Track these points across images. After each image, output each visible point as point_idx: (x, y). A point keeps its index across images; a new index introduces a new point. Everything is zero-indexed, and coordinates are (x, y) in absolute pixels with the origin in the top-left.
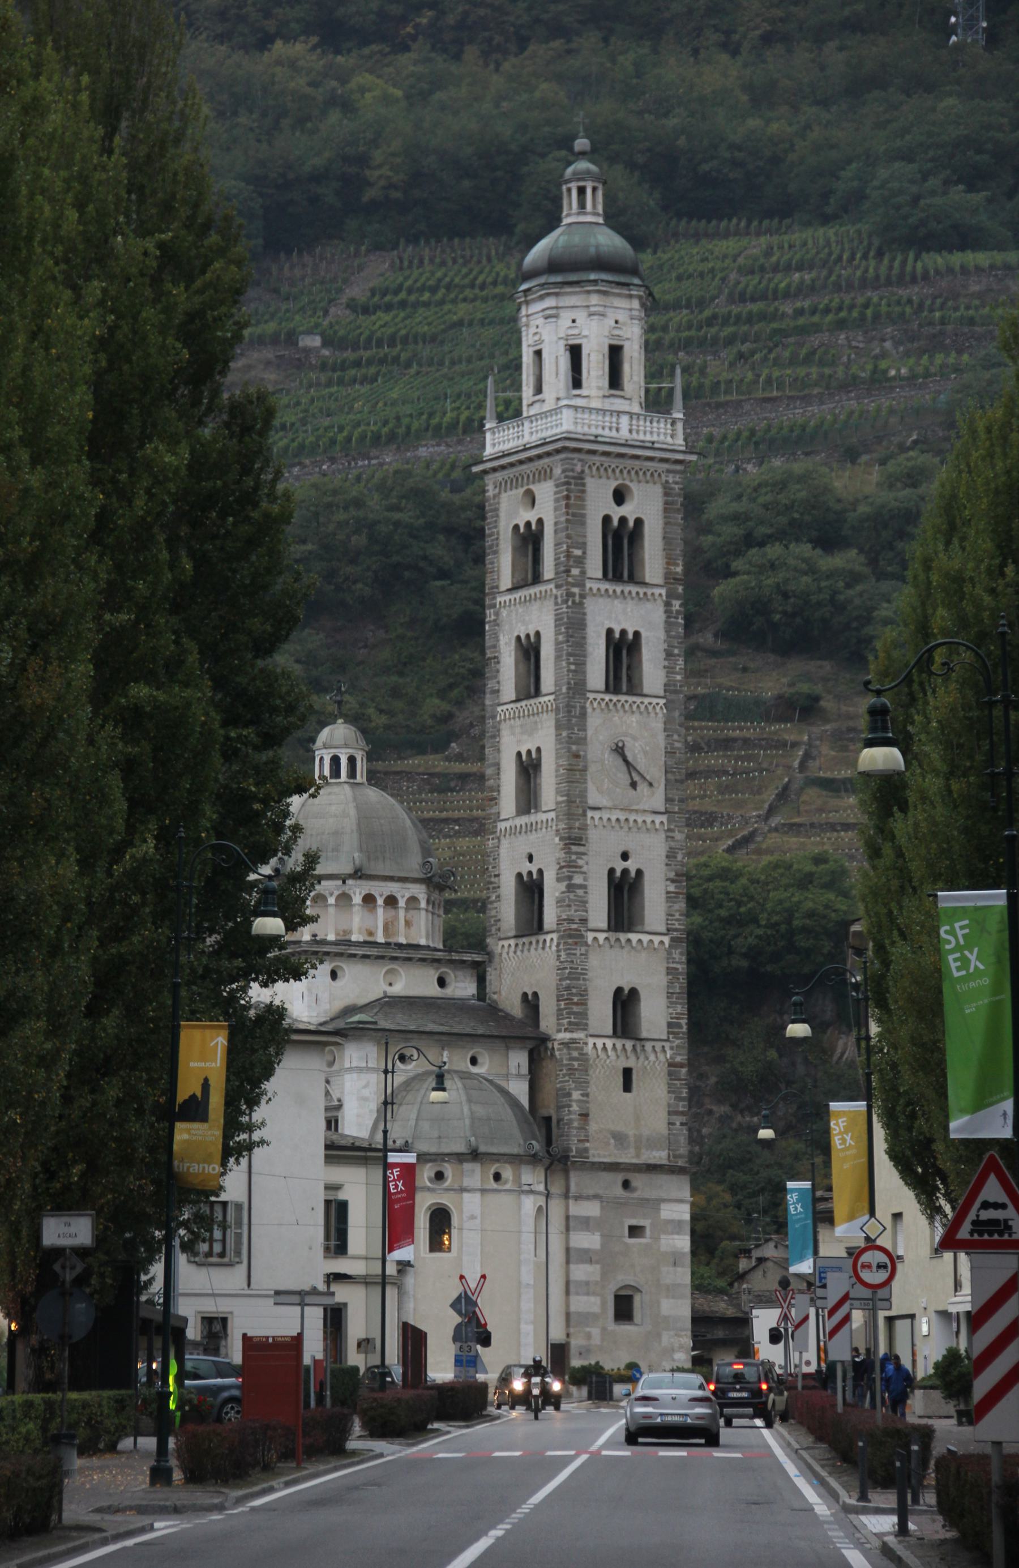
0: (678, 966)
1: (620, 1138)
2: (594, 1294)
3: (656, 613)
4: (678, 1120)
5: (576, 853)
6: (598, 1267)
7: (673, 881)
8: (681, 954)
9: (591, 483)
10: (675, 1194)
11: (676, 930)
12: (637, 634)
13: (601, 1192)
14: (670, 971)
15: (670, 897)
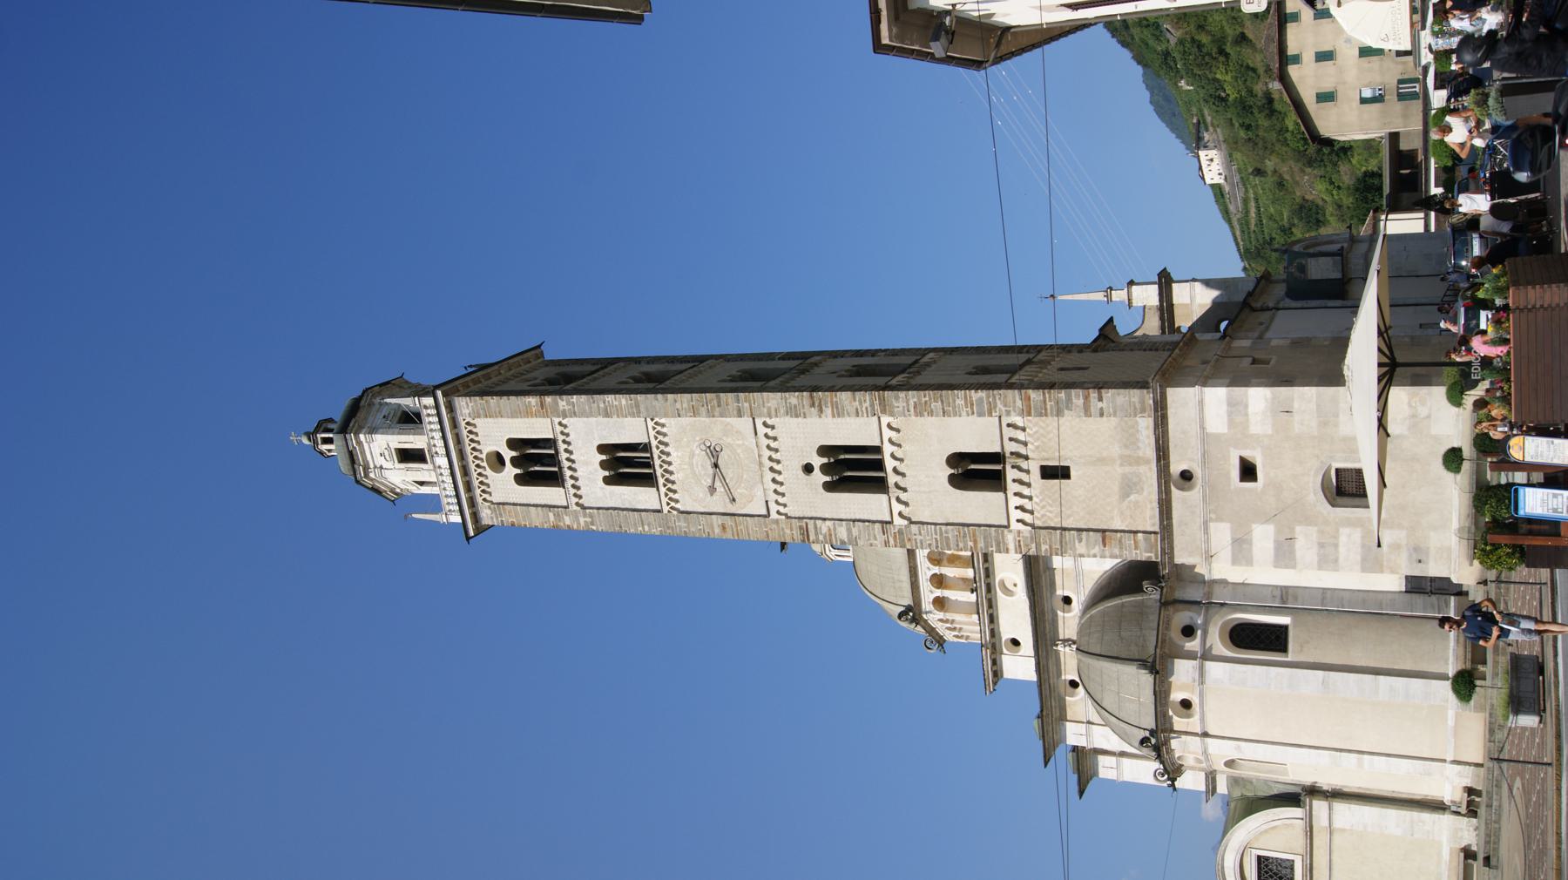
0: (911, 403)
1: (1128, 487)
2: (1336, 537)
3: (576, 426)
4: (1095, 405)
5: (816, 534)
6: (1298, 529)
7: (821, 411)
8: (897, 398)
9: (497, 497)
10: (1192, 412)
11: (872, 405)
12: (602, 449)
13: (1199, 521)
14: (919, 414)
15: (839, 412)
